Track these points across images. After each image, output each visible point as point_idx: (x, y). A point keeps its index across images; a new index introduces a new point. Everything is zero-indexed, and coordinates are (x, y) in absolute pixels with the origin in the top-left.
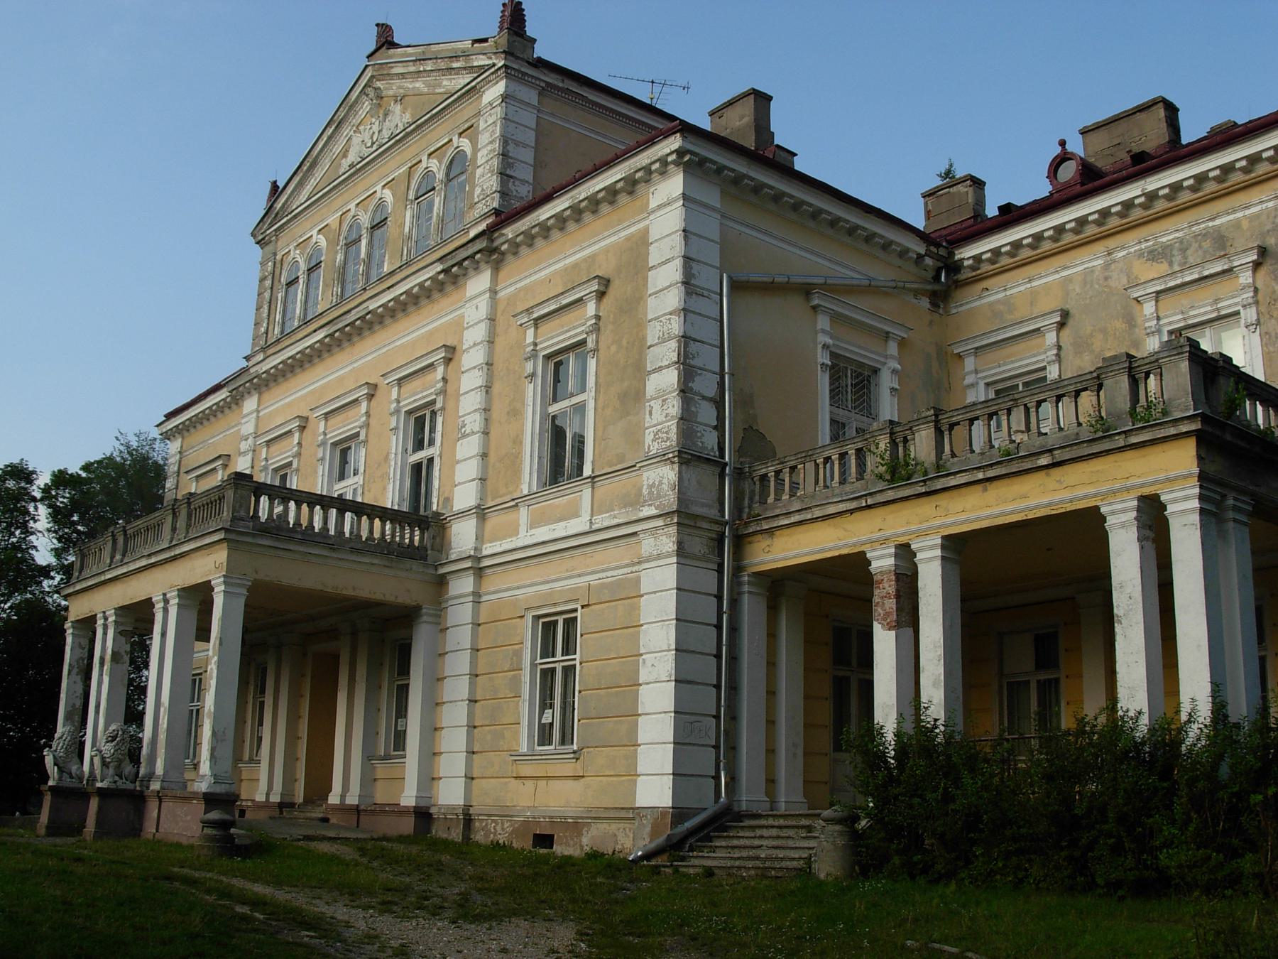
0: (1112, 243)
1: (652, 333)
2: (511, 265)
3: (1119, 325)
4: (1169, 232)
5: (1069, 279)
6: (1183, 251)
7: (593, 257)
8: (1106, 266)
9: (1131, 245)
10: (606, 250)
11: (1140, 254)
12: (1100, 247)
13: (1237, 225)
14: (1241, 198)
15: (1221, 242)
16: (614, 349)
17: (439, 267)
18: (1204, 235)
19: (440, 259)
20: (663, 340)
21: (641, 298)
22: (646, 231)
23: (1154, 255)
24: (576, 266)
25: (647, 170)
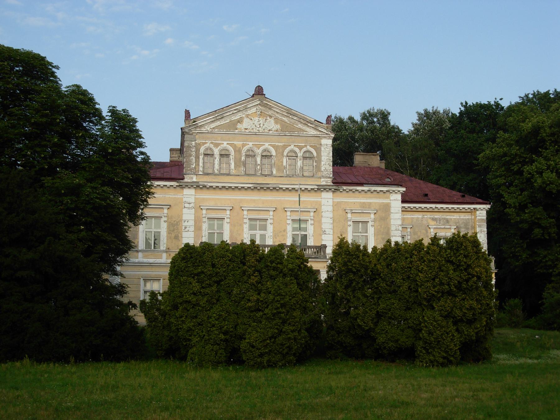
0: (424, 213)
1: (393, 228)
2: (338, 193)
3: (424, 231)
4: (437, 216)
5: (412, 218)
6: (440, 220)
7: (370, 203)
8: (422, 218)
9: (428, 215)
10: (375, 203)
11: (430, 218)
12: (421, 213)
13: (451, 219)
14: (453, 214)
15: (447, 221)
16: (379, 227)
17: (317, 187)
18: (445, 219)
19: (318, 185)
21: (387, 218)
22: (390, 203)
23: (434, 219)
24: (364, 203)
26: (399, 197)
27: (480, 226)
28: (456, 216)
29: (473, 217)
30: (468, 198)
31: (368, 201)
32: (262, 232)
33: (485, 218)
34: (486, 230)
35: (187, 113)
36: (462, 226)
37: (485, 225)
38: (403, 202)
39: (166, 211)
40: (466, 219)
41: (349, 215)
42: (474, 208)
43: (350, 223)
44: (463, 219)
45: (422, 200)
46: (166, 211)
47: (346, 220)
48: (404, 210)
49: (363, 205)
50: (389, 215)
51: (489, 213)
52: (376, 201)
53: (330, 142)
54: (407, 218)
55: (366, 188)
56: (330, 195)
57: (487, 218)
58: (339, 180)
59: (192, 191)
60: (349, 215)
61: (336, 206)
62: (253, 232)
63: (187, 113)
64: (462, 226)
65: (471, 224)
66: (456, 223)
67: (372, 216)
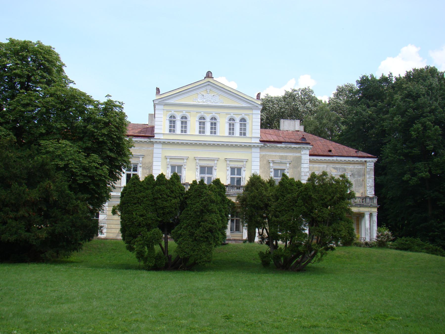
0: (328, 164)
1: (303, 174)
4: (338, 166)
6: (339, 169)
7: (287, 156)
8: (327, 167)
9: (331, 165)
10: (290, 156)
13: (348, 168)
14: (349, 165)
18: (343, 168)
20: (305, 176)
22: (301, 156)
23: (334, 168)
24: (282, 156)
25: (304, 148)
26: (308, 152)
27: (369, 174)
28: (351, 167)
29: (364, 167)
30: (361, 153)
31: (285, 155)
32: (209, 175)
33: (373, 168)
34: (373, 176)
35: (158, 90)
36: (356, 173)
37: (372, 173)
38: (310, 155)
39: (141, 159)
40: (359, 169)
41: (271, 165)
42: (365, 161)
43: (272, 170)
44: (357, 168)
45: (327, 154)
46: (141, 159)
47: (270, 167)
48: (311, 161)
49: (281, 157)
50: (300, 165)
51: (376, 165)
52: (291, 155)
53: (259, 112)
54: (316, 167)
55: (283, 145)
56: (258, 150)
57: (374, 168)
58: (265, 139)
59: (160, 146)
60: (271, 165)
61: (262, 158)
62: (203, 175)
63: (158, 90)
64: (356, 173)
65: (362, 172)
66: (351, 171)
67: (288, 165)
